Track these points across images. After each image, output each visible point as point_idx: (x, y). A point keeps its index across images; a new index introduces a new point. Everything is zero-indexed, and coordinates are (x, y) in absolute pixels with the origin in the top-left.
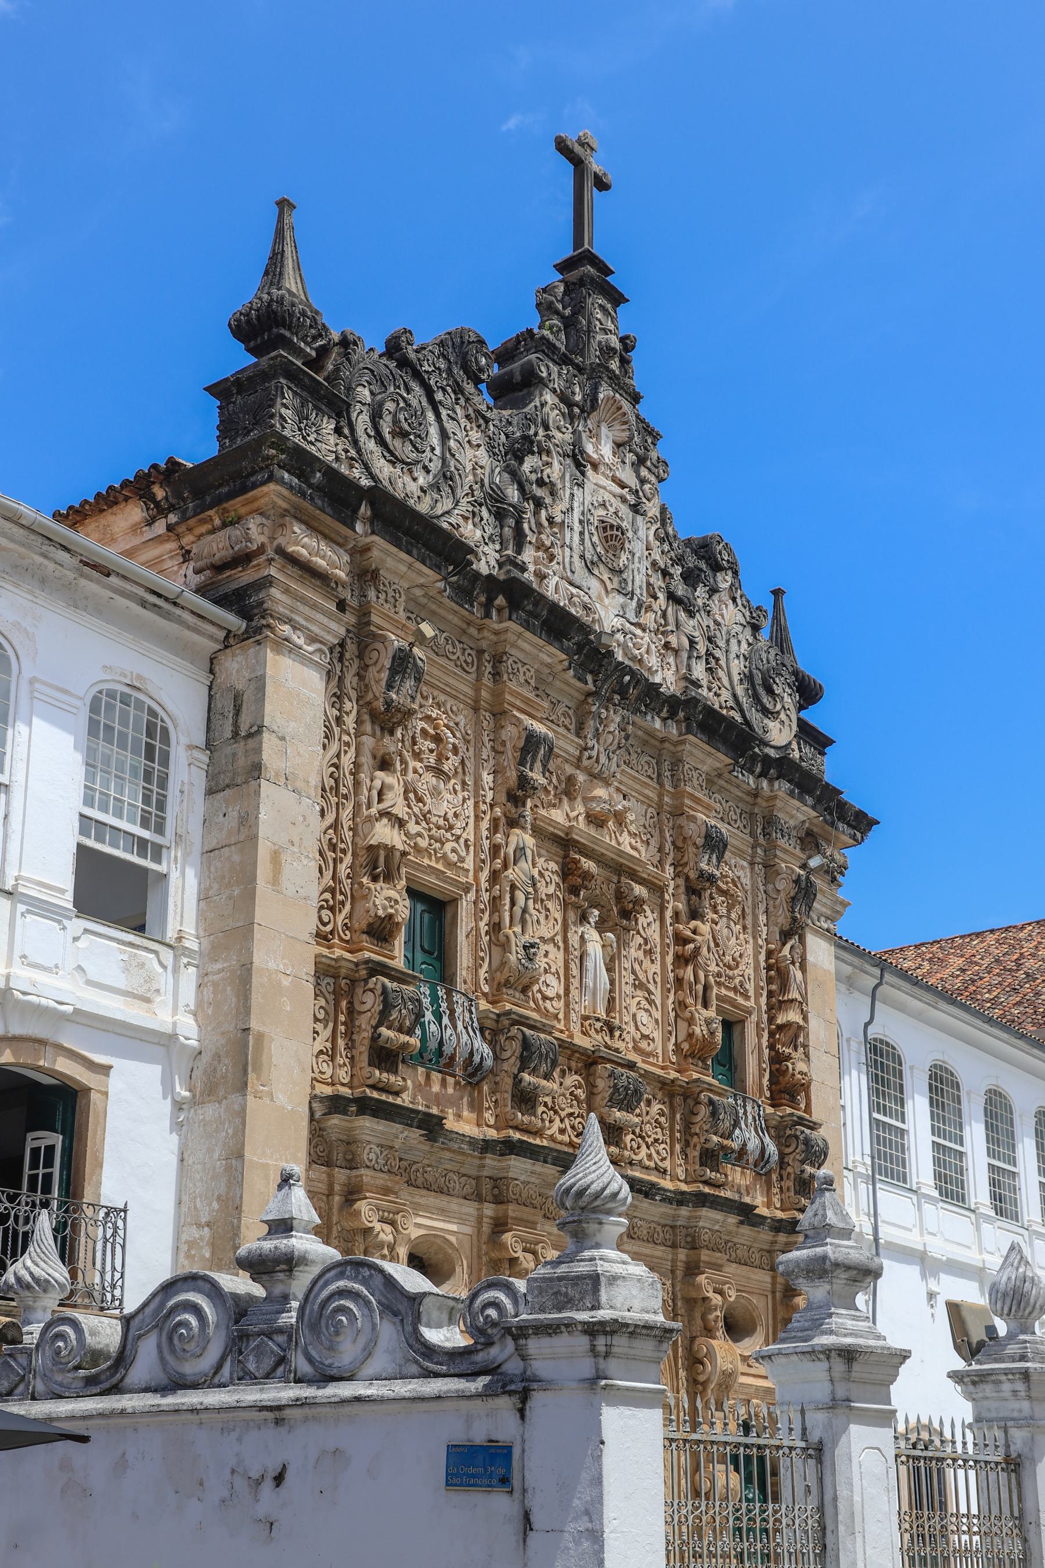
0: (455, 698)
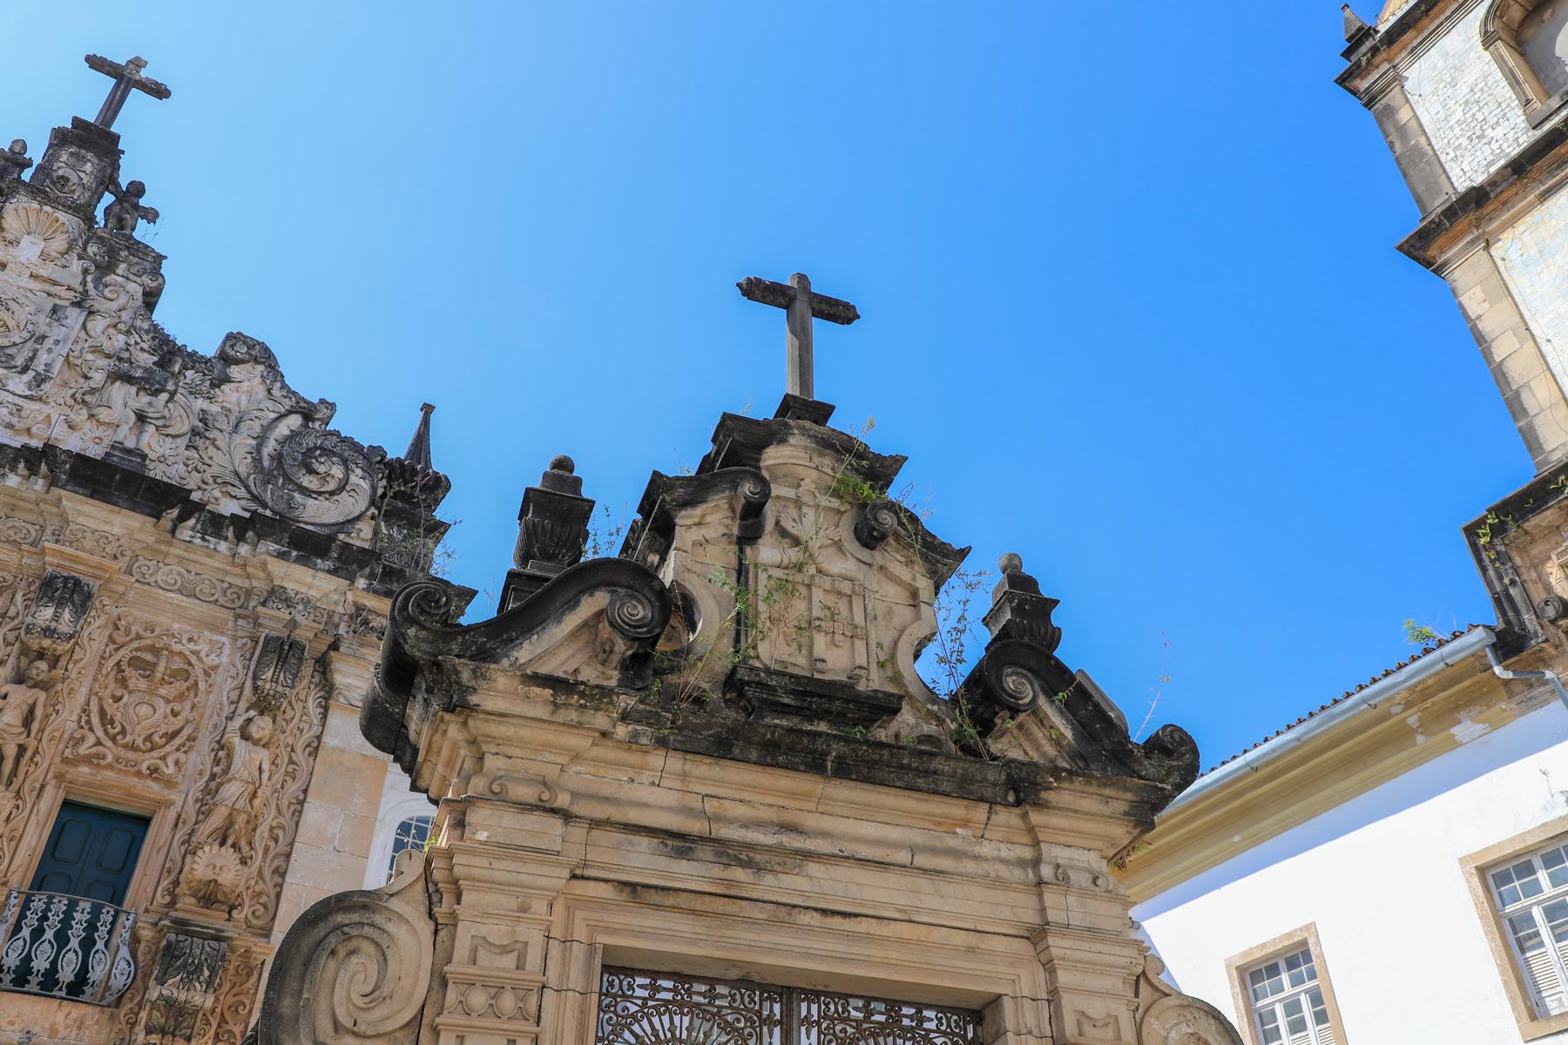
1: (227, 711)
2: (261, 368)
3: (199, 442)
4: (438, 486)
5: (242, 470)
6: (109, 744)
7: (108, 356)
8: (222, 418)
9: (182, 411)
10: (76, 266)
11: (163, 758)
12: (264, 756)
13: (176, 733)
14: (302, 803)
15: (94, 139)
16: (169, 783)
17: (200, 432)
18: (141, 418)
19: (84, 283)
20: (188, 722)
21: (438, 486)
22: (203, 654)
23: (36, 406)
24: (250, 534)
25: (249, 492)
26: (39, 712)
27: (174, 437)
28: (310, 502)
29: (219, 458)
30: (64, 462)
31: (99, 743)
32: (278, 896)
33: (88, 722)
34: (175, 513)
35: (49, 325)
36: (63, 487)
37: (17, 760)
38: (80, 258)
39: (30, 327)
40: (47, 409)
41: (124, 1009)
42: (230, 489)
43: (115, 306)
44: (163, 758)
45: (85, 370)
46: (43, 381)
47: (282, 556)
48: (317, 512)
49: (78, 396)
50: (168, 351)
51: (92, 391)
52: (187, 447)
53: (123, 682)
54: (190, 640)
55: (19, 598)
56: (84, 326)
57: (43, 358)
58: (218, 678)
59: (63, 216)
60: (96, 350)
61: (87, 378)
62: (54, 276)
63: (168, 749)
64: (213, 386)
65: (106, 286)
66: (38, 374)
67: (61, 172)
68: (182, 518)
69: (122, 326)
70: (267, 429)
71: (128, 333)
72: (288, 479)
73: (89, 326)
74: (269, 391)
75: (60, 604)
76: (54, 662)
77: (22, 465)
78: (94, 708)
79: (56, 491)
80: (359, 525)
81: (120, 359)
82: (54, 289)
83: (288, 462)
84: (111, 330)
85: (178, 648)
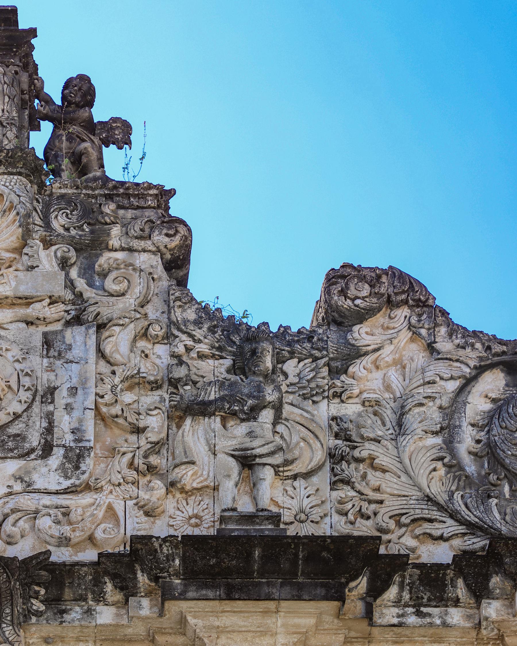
3: (350, 470)
7: (155, 386)
9: (303, 431)
17: (344, 452)
18: (247, 462)
25: (462, 522)
27: (307, 475)
29: (391, 484)
30: (170, 558)
34: (361, 585)
35: (51, 369)
36: (182, 597)
42: (427, 527)
43: (130, 301)
45: (132, 418)
46: (80, 457)
49: (139, 461)
50: (243, 344)
51: (156, 447)
52: (333, 486)
56: (101, 353)
61: (138, 431)
66: (68, 449)
68: (376, 591)
69: (156, 330)
71: (168, 338)
73: (108, 349)
77: (109, 587)
79: (174, 607)
81: (174, 383)
82: (36, 310)
84: (142, 344)
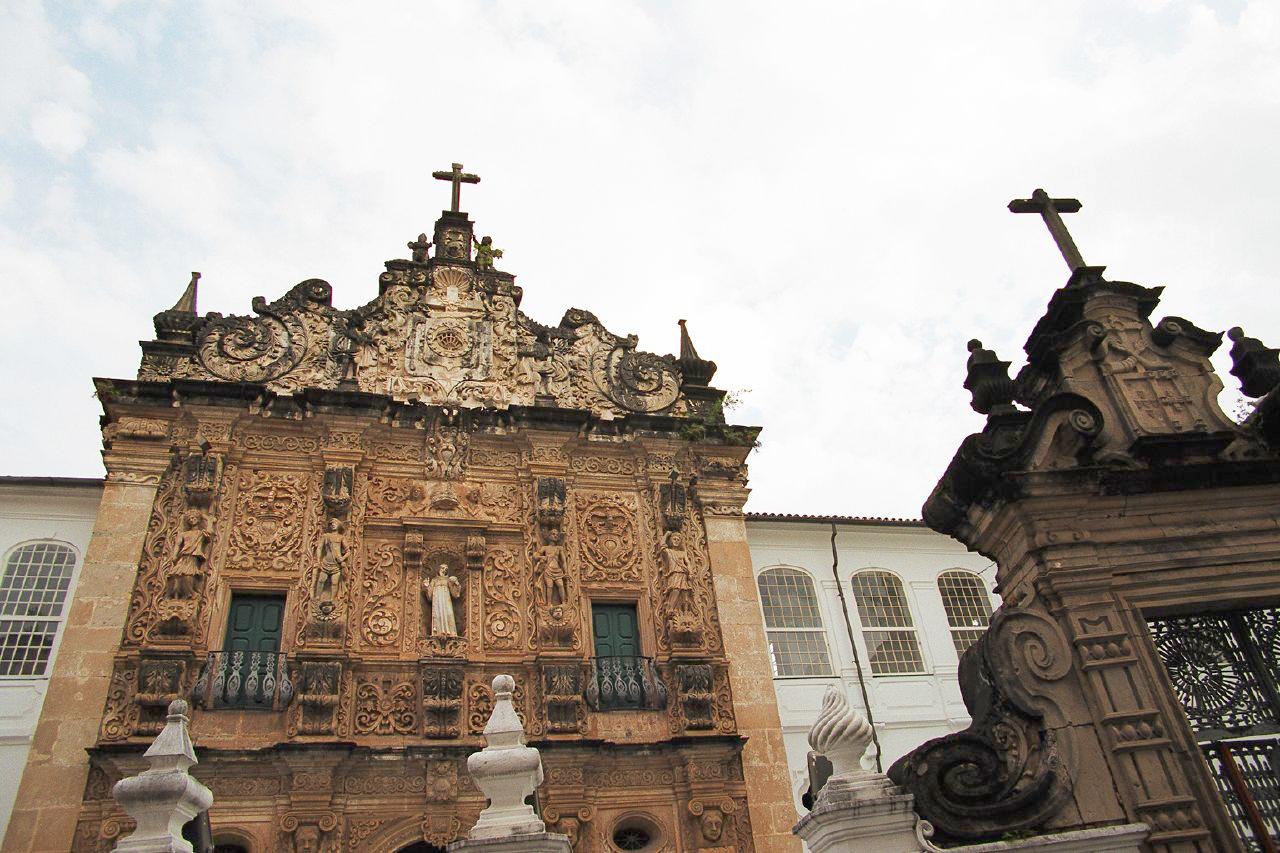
0: (297, 470)
1: (652, 533)
2: (590, 326)
4: (709, 369)
5: (605, 389)
6: (601, 568)
7: (512, 344)
8: (582, 363)
9: (560, 364)
10: (477, 295)
11: (630, 569)
12: (683, 554)
13: (631, 553)
14: (711, 577)
15: (454, 221)
16: (637, 582)
17: (574, 375)
18: (544, 375)
19: (485, 306)
20: (634, 545)
21: (709, 369)
22: (626, 505)
23: (490, 384)
24: (628, 428)
25: (614, 402)
26: (564, 558)
28: (648, 399)
29: (591, 386)
31: (596, 568)
32: (720, 632)
33: (586, 558)
37: (565, 588)
38: (477, 290)
39: (471, 340)
40: (496, 385)
41: (670, 709)
44: (630, 569)
47: (650, 436)
48: (654, 403)
53: (593, 530)
54: (617, 498)
55: (525, 496)
57: (483, 356)
58: (639, 517)
59: (461, 270)
60: (505, 342)
62: (470, 307)
63: (631, 563)
64: (571, 344)
65: (495, 303)
67: (451, 245)
70: (608, 361)
71: (515, 327)
72: (632, 389)
74: (600, 339)
75: (551, 495)
76: (558, 526)
78: (585, 549)
80: (678, 404)
81: (519, 344)
83: (626, 378)
85: (612, 505)
